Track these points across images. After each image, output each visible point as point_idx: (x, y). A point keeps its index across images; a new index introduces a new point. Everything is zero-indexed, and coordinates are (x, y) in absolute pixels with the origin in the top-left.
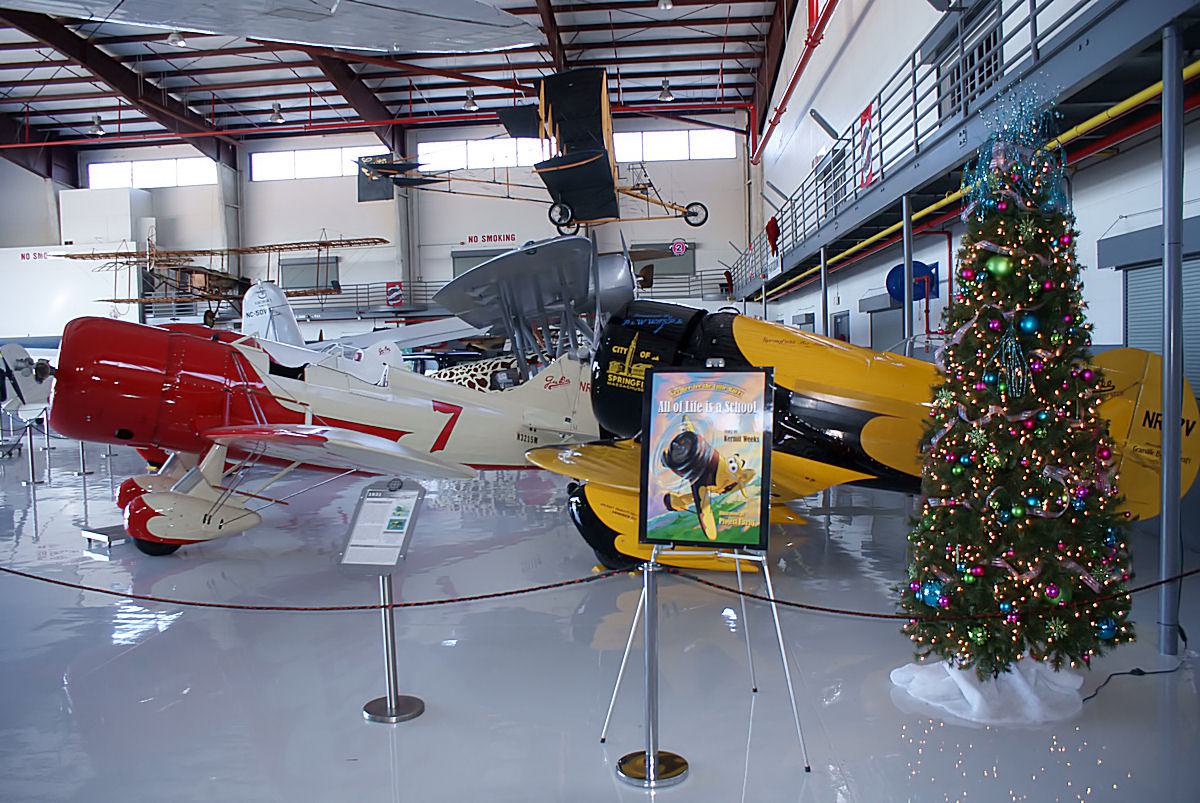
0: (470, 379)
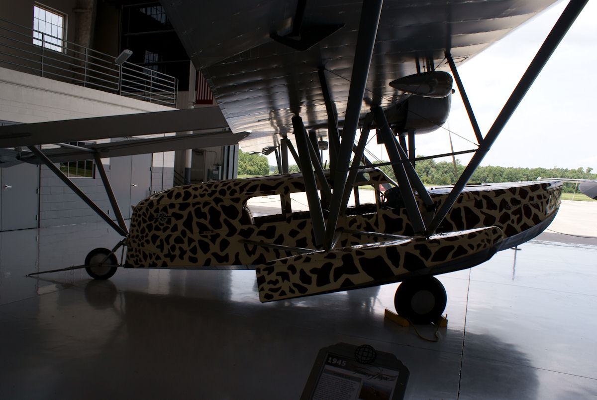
0: (213, 204)
